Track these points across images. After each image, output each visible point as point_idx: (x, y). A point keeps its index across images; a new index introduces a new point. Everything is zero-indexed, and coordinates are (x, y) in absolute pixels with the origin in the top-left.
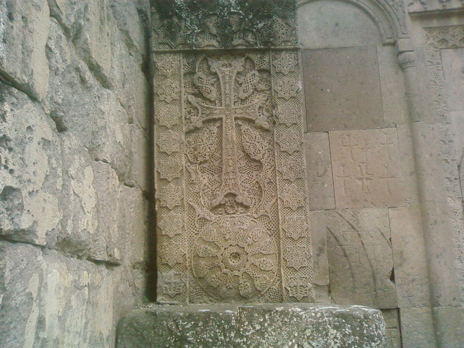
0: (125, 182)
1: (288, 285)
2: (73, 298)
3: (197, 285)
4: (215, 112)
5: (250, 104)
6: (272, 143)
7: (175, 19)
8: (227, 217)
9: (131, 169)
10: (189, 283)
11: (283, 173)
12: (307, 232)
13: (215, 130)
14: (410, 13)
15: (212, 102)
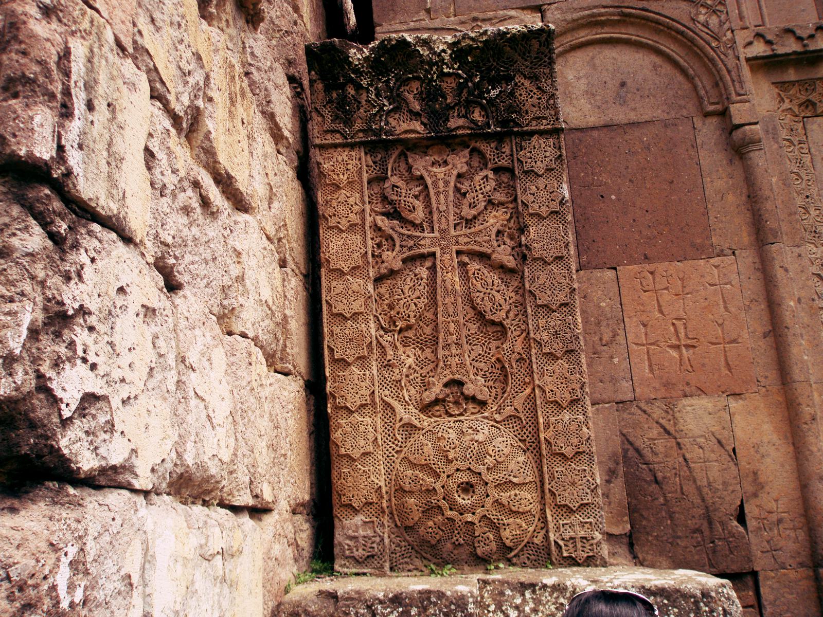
1: (560, 537)
2: (198, 576)
4: (422, 242)
5: (481, 227)
6: (521, 291)
7: (349, 90)
9: (286, 346)
10: (389, 537)
13: (424, 273)
14: (748, 60)
15: (417, 225)
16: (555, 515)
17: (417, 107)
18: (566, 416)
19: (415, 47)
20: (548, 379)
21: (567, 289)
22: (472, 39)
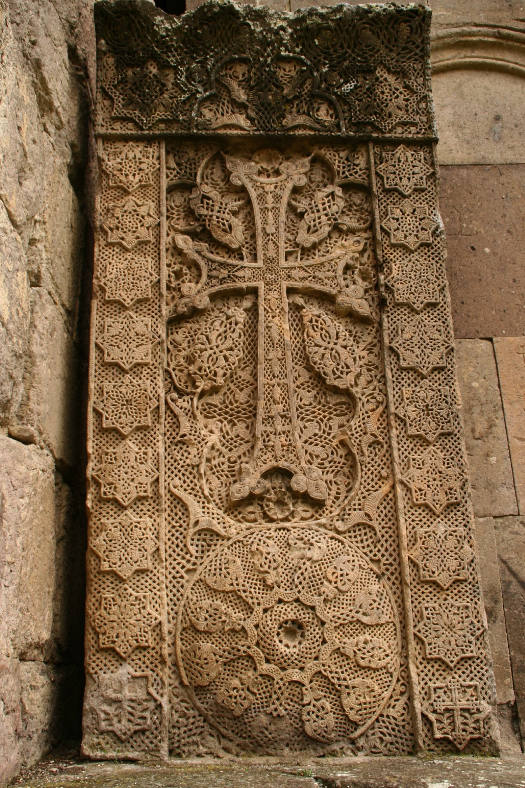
0: (11, 428)
1: (431, 708)
3: (191, 704)
4: (240, 274)
5: (323, 259)
6: (376, 350)
7: (151, 68)
8: (269, 529)
9: (28, 399)
10: (170, 702)
11: (407, 419)
12: (471, 569)
16: (422, 675)
17: (242, 96)
18: (441, 528)
19: (245, 20)
20: (414, 472)
21: (443, 348)
22: (322, 16)
